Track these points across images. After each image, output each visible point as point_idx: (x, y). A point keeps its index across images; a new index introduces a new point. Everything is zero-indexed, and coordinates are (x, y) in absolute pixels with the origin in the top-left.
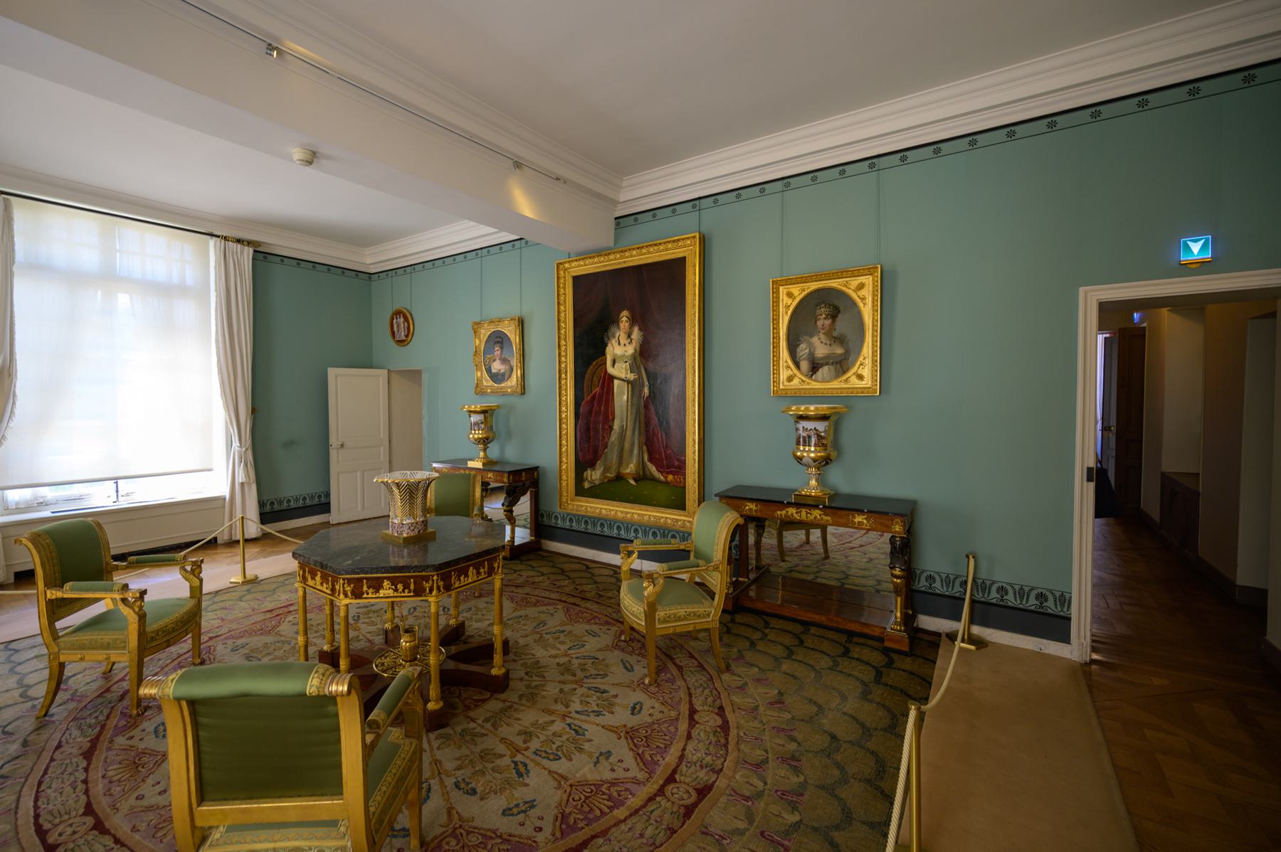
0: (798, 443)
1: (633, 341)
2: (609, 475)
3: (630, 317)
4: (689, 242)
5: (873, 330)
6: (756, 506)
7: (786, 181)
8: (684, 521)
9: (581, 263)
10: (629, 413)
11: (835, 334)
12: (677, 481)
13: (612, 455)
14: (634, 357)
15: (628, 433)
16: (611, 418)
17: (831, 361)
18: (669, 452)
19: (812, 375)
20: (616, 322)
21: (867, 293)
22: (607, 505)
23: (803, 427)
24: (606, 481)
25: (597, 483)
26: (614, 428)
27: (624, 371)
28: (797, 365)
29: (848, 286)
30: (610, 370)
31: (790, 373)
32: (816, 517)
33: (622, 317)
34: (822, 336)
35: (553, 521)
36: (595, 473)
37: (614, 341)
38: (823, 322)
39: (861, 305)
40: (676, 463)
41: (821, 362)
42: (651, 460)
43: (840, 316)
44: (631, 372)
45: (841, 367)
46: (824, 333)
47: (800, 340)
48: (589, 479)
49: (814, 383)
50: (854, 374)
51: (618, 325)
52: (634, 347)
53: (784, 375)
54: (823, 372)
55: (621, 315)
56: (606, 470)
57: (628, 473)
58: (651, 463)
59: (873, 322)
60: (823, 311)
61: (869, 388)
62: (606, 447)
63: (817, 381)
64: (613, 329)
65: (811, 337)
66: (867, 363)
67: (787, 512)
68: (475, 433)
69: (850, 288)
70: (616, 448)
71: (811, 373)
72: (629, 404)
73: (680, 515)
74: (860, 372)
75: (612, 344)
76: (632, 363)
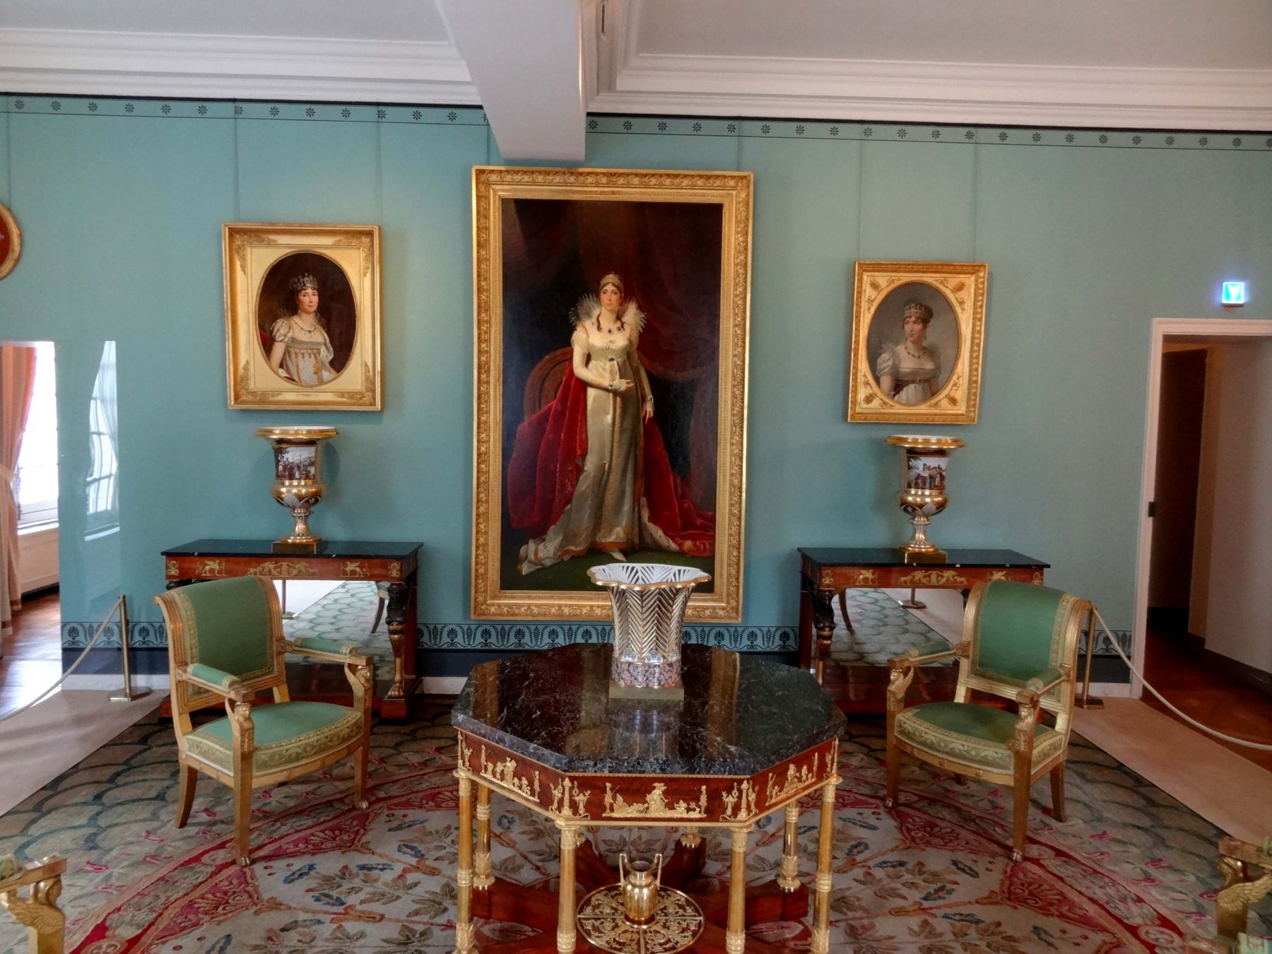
0: (910, 486)
1: (625, 326)
2: (573, 548)
3: (621, 286)
4: (732, 183)
5: (972, 343)
6: (873, 574)
7: (866, 126)
8: (714, 608)
9: (526, 178)
10: (615, 445)
11: (925, 344)
12: (698, 550)
13: (580, 515)
14: (627, 353)
15: (612, 477)
16: (579, 452)
17: (918, 378)
18: (686, 505)
19: (894, 395)
20: (594, 291)
21: (968, 295)
22: (570, 598)
23: (925, 465)
24: (566, 558)
25: (548, 563)
26: (586, 468)
27: (607, 375)
28: (877, 380)
29: (947, 284)
30: (580, 370)
31: (869, 391)
32: (948, 580)
33: (605, 285)
34: (909, 344)
35: (445, 639)
36: (545, 547)
37: (589, 324)
38: (912, 327)
39: (958, 310)
40: (699, 522)
41: (905, 379)
42: (653, 519)
43: (932, 321)
44: (621, 378)
45: (931, 387)
46: (911, 341)
47: (882, 348)
48: (532, 557)
49: (898, 406)
50: (946, 396)
51: (598, 296)
52: (628, 336)
53: (862, 393)
54: (908, 392)
55: (603, 281)
56: (568, 538)
57: (612, 543)
58: (655, 524)
59: (973, 333)
60: (912, 313)
61: (962, 415)
62: (569, 501)
63: (901, 404)
64: (588, 302)
65: (897, 344)
66: (961, 383)
67: (914, 577)
68: (291, 485)
69: (947, 287)
70: (589, 502)
71: (893, 393)
72: (617, 429)
73: (705, 600)
74: (952, 394)
75: (584, 327)
76: (624, 362)
